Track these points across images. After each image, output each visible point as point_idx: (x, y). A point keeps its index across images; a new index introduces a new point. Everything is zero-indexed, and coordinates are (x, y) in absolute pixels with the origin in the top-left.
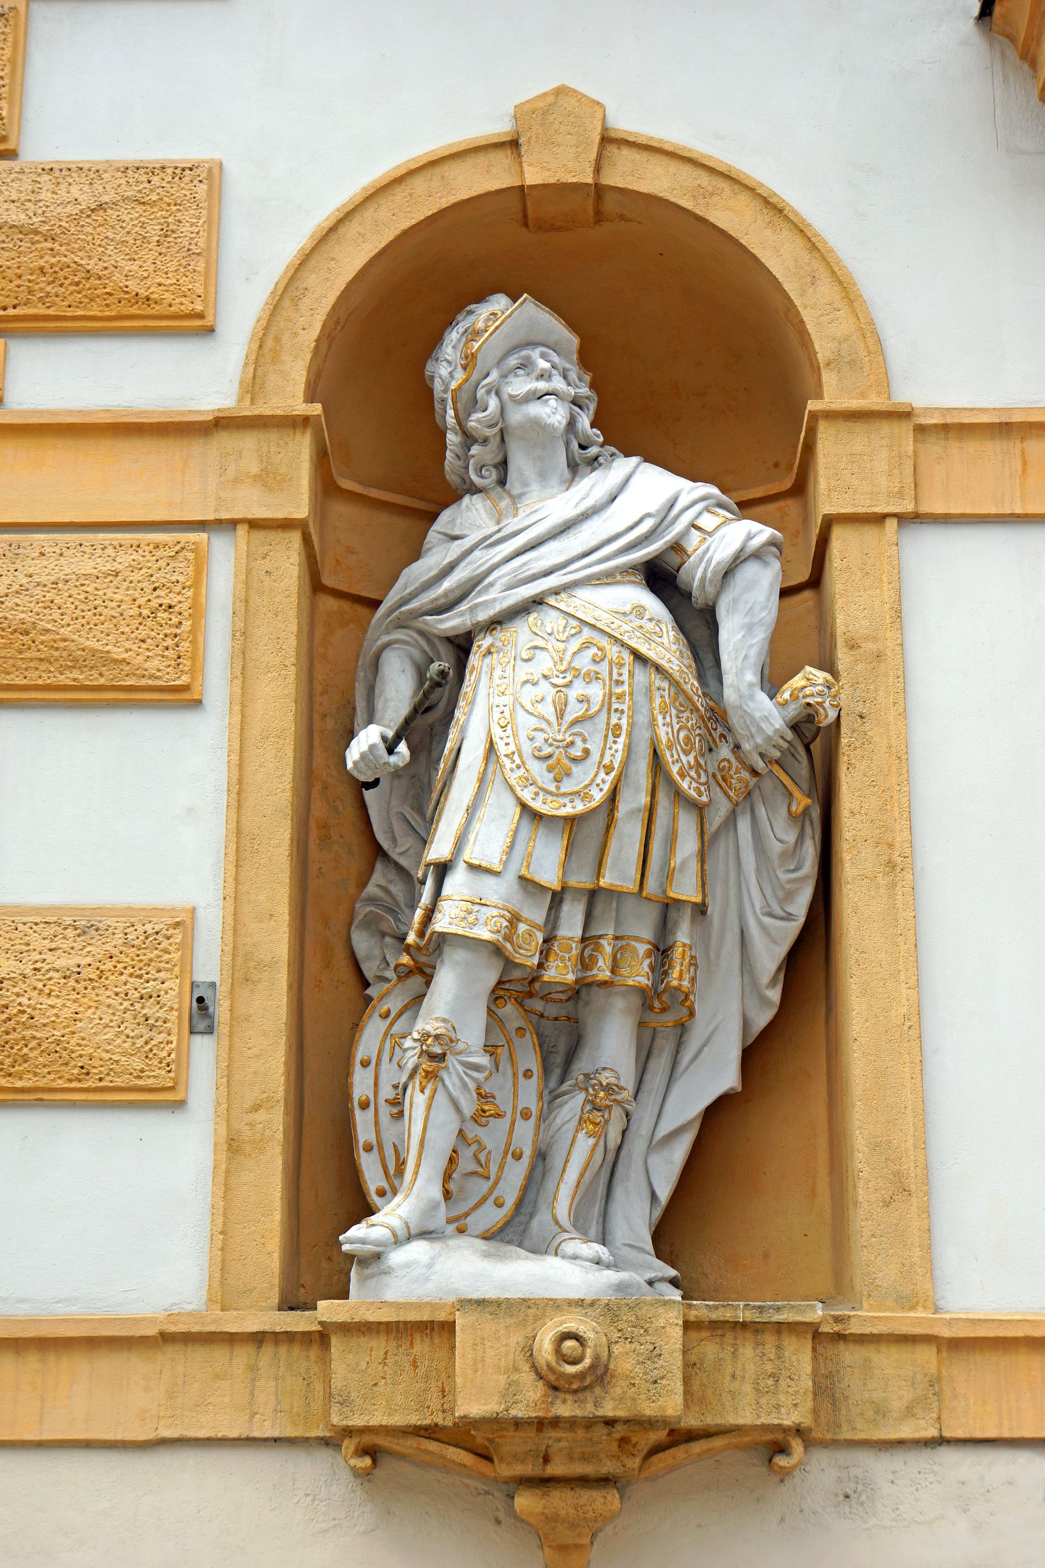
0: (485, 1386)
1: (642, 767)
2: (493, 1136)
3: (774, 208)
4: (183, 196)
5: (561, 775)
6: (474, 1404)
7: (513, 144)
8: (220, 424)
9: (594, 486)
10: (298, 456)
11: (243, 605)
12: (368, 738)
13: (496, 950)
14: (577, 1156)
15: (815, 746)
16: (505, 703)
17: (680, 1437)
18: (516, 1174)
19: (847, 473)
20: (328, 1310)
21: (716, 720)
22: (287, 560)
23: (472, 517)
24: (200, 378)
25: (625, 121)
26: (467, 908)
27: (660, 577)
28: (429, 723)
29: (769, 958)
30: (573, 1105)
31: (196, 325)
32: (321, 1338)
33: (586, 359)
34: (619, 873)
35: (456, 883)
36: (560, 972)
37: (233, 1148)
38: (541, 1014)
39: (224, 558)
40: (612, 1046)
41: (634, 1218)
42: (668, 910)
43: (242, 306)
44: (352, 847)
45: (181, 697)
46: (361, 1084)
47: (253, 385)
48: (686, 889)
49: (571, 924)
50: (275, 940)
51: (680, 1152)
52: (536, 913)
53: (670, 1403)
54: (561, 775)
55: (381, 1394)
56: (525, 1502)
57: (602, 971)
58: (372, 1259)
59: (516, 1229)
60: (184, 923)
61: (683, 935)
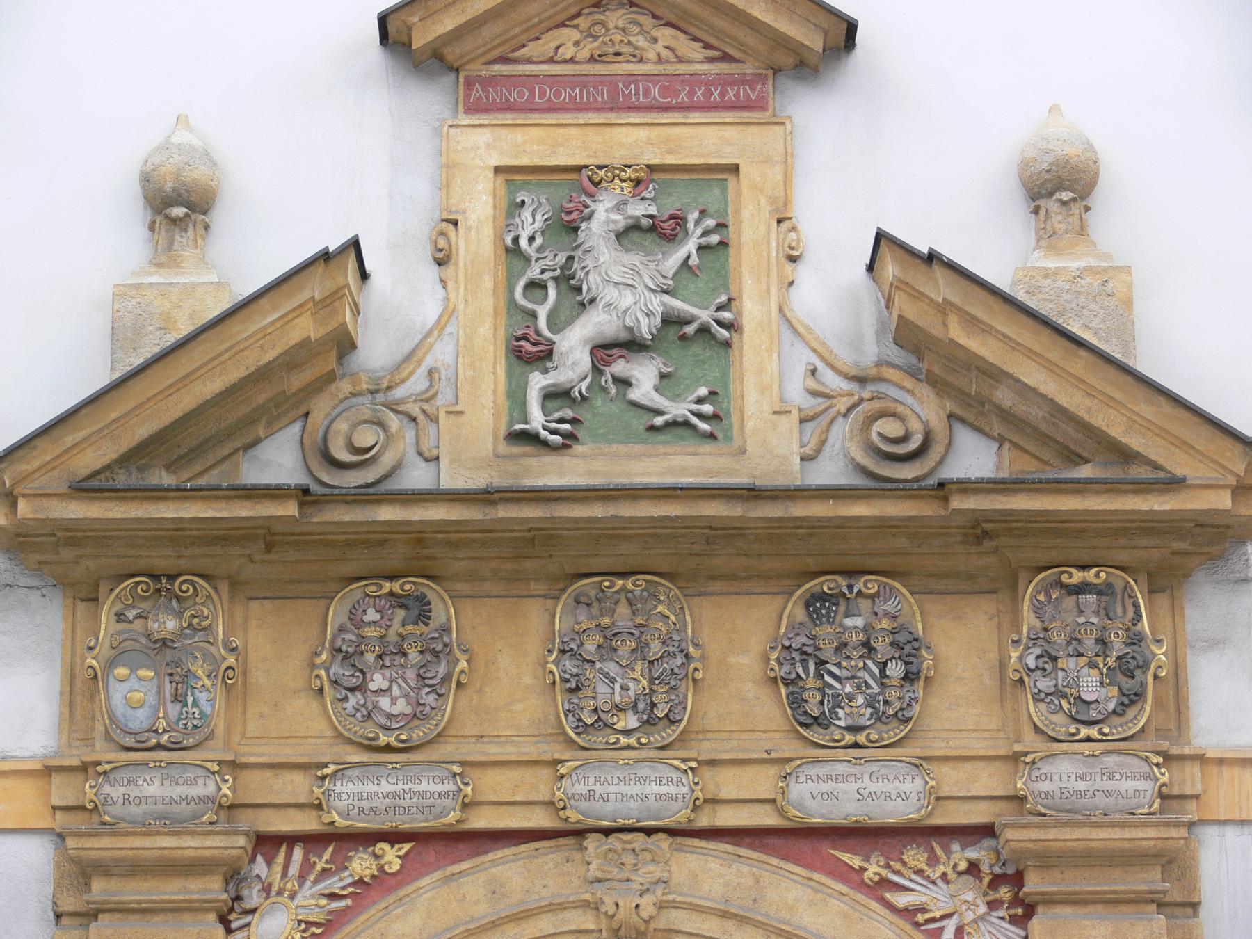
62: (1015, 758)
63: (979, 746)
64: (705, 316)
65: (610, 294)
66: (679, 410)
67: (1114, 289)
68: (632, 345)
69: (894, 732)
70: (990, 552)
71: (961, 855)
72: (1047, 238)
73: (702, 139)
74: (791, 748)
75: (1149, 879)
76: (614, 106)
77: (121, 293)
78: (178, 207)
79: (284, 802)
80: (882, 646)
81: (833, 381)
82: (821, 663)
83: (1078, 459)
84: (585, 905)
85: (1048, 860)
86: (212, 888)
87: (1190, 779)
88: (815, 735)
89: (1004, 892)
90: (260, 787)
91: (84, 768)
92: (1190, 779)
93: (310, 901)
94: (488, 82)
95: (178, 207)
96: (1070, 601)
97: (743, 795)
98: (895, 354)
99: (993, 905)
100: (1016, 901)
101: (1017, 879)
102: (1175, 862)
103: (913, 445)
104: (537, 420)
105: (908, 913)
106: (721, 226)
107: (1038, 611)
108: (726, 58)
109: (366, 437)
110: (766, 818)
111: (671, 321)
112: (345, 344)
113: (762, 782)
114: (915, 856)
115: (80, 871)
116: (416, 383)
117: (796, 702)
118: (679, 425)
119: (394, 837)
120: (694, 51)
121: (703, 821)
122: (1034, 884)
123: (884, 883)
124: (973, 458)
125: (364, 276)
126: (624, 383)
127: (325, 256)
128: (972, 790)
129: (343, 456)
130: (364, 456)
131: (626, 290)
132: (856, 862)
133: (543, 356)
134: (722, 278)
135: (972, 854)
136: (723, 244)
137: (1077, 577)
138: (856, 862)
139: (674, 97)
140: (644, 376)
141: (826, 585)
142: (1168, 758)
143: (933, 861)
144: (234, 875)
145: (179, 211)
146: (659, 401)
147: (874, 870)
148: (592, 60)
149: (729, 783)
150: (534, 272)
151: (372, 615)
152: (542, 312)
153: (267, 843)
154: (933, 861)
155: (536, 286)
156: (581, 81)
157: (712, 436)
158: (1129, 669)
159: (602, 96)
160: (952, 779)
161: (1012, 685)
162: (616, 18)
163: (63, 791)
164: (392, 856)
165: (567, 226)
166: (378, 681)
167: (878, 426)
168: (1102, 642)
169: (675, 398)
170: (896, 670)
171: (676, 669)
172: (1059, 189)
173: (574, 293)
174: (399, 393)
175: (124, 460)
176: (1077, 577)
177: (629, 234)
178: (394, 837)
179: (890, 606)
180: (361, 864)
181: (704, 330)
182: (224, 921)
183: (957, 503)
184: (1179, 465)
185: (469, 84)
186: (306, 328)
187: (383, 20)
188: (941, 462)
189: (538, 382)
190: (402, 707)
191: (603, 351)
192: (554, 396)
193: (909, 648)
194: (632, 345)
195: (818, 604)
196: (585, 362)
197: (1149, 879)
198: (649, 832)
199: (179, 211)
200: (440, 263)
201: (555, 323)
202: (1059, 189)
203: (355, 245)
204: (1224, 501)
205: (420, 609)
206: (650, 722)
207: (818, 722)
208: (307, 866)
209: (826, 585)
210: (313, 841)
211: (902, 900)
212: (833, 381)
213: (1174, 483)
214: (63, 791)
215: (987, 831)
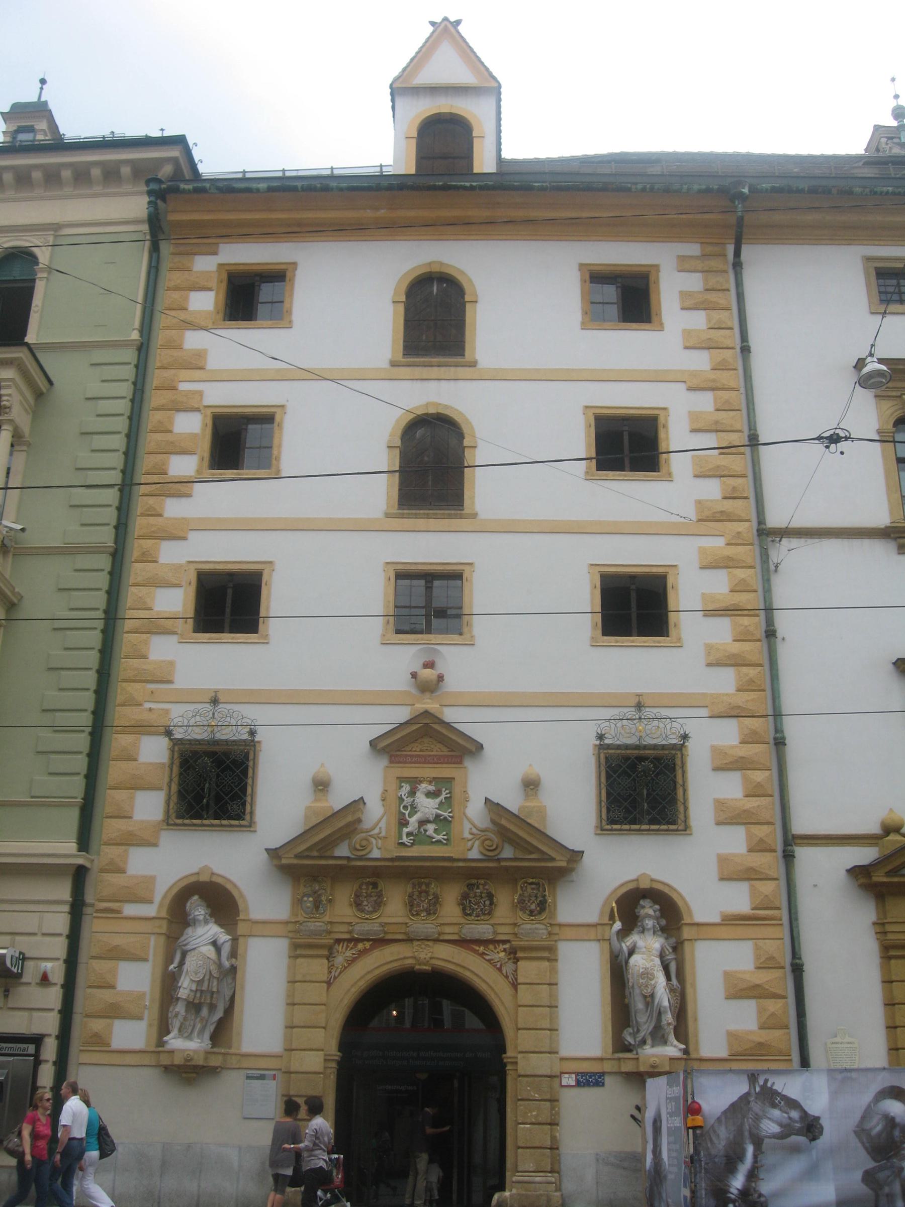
0: (178, 1060)
1: (208, 973)
2: (187, 1023)
3: (235, 886)
4: (149, 881)
5: (196, 974)
6: (176, 1062)
7: (198, 873)
8: (154, 918)
9: (207, 928)
10: (164, 924)
11: (155, 946)
12: (171, 967)
13: (185, 999)
14: (199, 1026)
15: (233, 969)
16: (191, 963)
17: (203, 1067)
18: (190, 1028)
19: (242, 928)
20: (160, 1049)
21: (220, 965)
22: (162, 939)
23: (189, 931)
24: (150, 911)
25: (216, 871)
26: (183, 993)
27: (214, 943)
28: (182, 963)
29: (227, 998)
30: (198, 1019)
31: (150, 902)
32: (159, 1052)
33: (208, 906)
34: (205, 987)
35: (181, 990)
36: (197, 1001)
37: (150, 1025)
38: (194, 1007)
39: (153, 938)
40: (205, 1012)
41: (207, 1035)
42: (213, 993)
43: (158, 898)
44: (169, 983)
45: (146, 960)
46: (170, 1015)
47: (159, 911)
48: (215, 989)
49: (198, 995)
50: (157, 996)
51: (214, 1025)
52: (192, 994)
53: (201, 1063)
54: (196, 974)
55: (165, 1060)
56: (184, 1075)
57: (202, 1001)
58: (166, 1042)
59: (189, 1037)
60: (144, 994)
61: (215, 996)
62: (515, 925)
63: (508, 921)
64: (446, 814)
65: (422, 809)
66: (440, 837)
67: (542, 812)
68: (428, 821)
69: (487, 917)
70: (511, 875)
71: (502, 947)
72: (527, 796)
73: (445, 771)
74: (463, 921)
75: (546, 954)
76: (425, 763)
77: (308, 808)
78: (321, 785)
79: (341, 932)
80: (483, 895)
81: (474, 830)
82: (470, 902)
83: (531, 853)
84: (412, 957)
85: (524, 949)
86: (326, 952)
87: (556, 930)
88: (469, 918)
89: (512, 956)
90: (337, 928)
91: (296, 922)
92: (556, 930)
93: (349, 954)
94: (397, 756)
95: (321, 785)
96: (529, 887)
97: (450, 932)
98: (490, 826)
99: (509, 959)
100: (515, 958)
101: (515, 953)
102: (552, 949)
103: (494, 847)
104: (405, 839)
105: (489, 961)
106: (450, 793)
107: (522, 888)
108: (452, 751)
109: (364, 843)
110: (456, 937)
111: (438, 816)
112: (359, 821)
113: (454, 929)
114: (491, 947)
115: (295, 946)
116: (376, 831)
117: (464, 909)
118: (439, 842)
119: (368, 940)
120: (445, 749)
121: (441, 938)
122: (519, 954)
123: (484, 953)
124: (508, 852)
125: (365, 804)
126: (426, 831)
127: (355, 801)
128: (504, 932)
129: (359, 848)
130: (364, 848)
131: (427, 806)
132: (477, 948)
133: (406, 824)
134: (450, 806)
135: (505, 946)
136: (450, 797)
137: (531, 880)
138: (477, 948)
139: (439, 760)
140: (431, 828)
141: (474, 881)
142: (551, 925)
143: (495, 948)
144: (330, 948)
145: (320, 788)
146: (435, 835)
147: (482, 949)
148: (421, 751)
149: (448, 929)
150: (405, 803)
151: (364, 887)
152: (407, 813)
153: (338, 941)
154: (495, 948)
155: (405, 807)
156: (418, 756)
157: (446, 844)
158: (542, 906)
159: (423, 760)
160: (501, 929)
161: (514, 907)
162: (426, 740)
163: (291, 927)
164: (368, 945)
165: (412, 793)
166: (365, 903)
167: (487, 842)
168: (536, 897)
169: (438, 834)
170: (487, 903)
171: (436, 901)
172: (531, 785)
173: (414, 809)
174: (372, 833)
175: (307, 850)
176: (531, 880)
177: (429, 794)
178: (368, 940)
179: (487, 887)
180: (360, 946)
181: (445, 818)
182: (328, 959)
183: (503, 864)
184: (553, 854)
185: (391, 756)
186: (350, 819)
187: (370, 742)
188: (499, 854)
189: (405, 830)
190: (371, 909)
191: (422, 823)
192: (409, 834)
193: (490, 896)
194: (428, 821)
195: (470, 886)
196: (417, 825)
197: (546, 954)
198: (428, 940)
199: (320, 788)
200: (383, 800)
201: (410, 815)
202: (531, 785)
203: (362, 798)
204: (564, 864)
205: (375, 885)
206: (429, 914)
207: (470, 915)
208: (348, 946)
209: (474, 881)
210: (349, 941)
211: (487, 957)
212: (474, 830)
213: (553, 859)
214: (291, 927)
215: (508, 941)
